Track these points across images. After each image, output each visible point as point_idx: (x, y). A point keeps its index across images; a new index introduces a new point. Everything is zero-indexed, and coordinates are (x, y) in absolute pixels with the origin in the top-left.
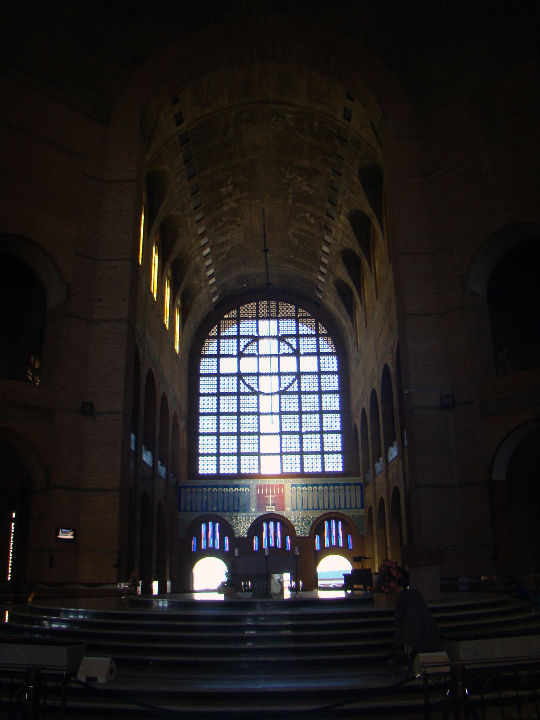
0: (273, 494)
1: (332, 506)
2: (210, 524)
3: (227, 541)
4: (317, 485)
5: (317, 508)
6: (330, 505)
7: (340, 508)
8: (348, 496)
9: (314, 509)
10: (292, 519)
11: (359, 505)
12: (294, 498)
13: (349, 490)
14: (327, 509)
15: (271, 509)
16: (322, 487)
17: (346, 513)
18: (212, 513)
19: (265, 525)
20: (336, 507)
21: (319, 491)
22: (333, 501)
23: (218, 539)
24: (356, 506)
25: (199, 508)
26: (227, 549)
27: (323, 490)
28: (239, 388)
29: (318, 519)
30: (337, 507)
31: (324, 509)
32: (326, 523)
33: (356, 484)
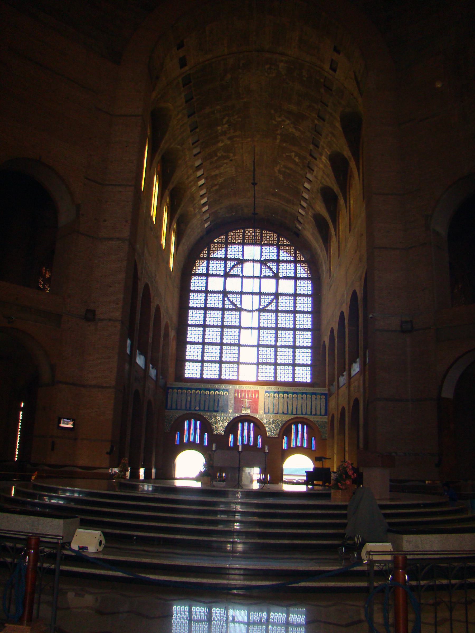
0: (248, 398)
1: (299, 412)
2: (193, 421)
4: (287, 393)
5: (286, 413)
7: (306, 414)
8: (314, 403)
9: (283, 413)
10: (264, 421)
11: (323, 412)
12: (267, 403)
13: (315, 399)
14: (295, 414)
15: (246, 411)
16: (292, 395)
17: (312, 418)
18: (195, 412)
19: (240, 425)
20: (303, 413)
21: (289, 398)
22: (301, 407)
23: (199, 434)
24: (321, 412)
25: (184, 407)
26: (206, 444)
27: (293, 398)
28: (224, 304)
29: (287, 422)
30: (304, 413)
31: (293, 414)
32: (293, 427)
33: (322, 394)
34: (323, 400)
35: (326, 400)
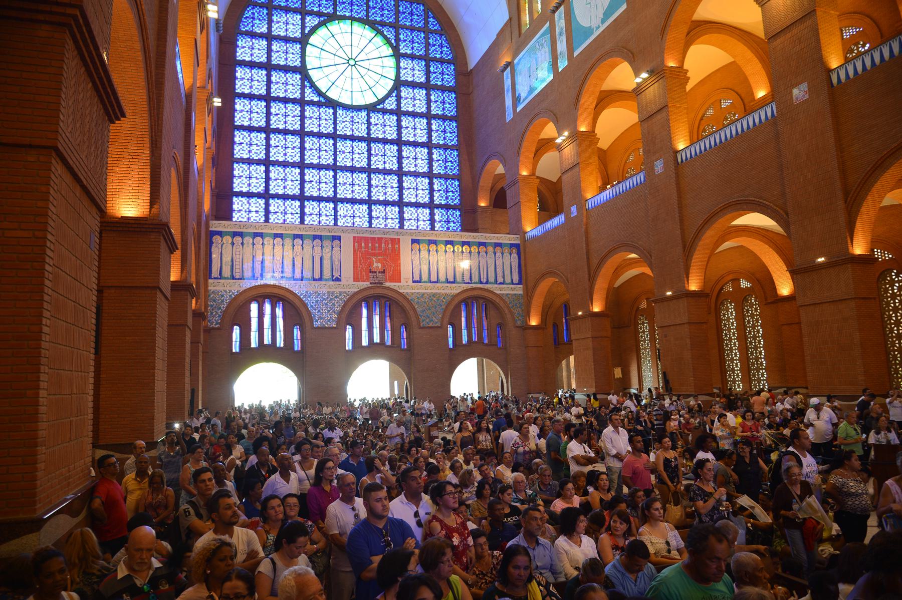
1: (475, 278)
3: (297, 333)
5: (452, 280)
6: (473, 275)
7: (487, 283)
8: (499, 263)
9: (447, 282)
11: (516, 279)
13: (501, 255)
14: (469, 283)
16: (460, 248)
20: (482, 280)
21: (455, 253)
22: (478, 269)
23: (282, 329)
24: (512, 280)
25: (248, 273)
26: (297, 347)
27: (463, 252)
28: (303, 93)
33: (512, 245)
34: (515, 256)
35: (519, 254)
